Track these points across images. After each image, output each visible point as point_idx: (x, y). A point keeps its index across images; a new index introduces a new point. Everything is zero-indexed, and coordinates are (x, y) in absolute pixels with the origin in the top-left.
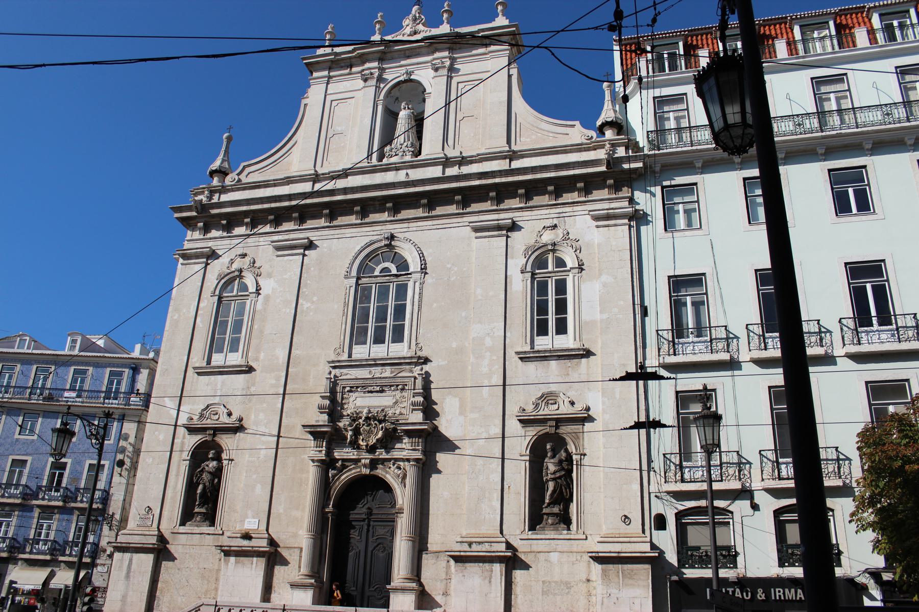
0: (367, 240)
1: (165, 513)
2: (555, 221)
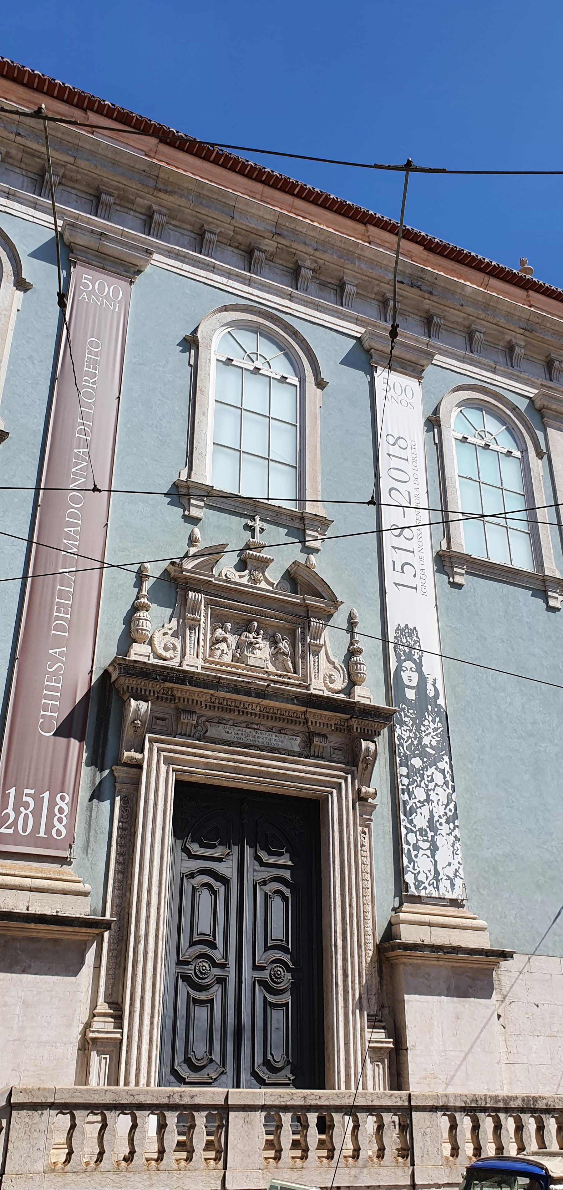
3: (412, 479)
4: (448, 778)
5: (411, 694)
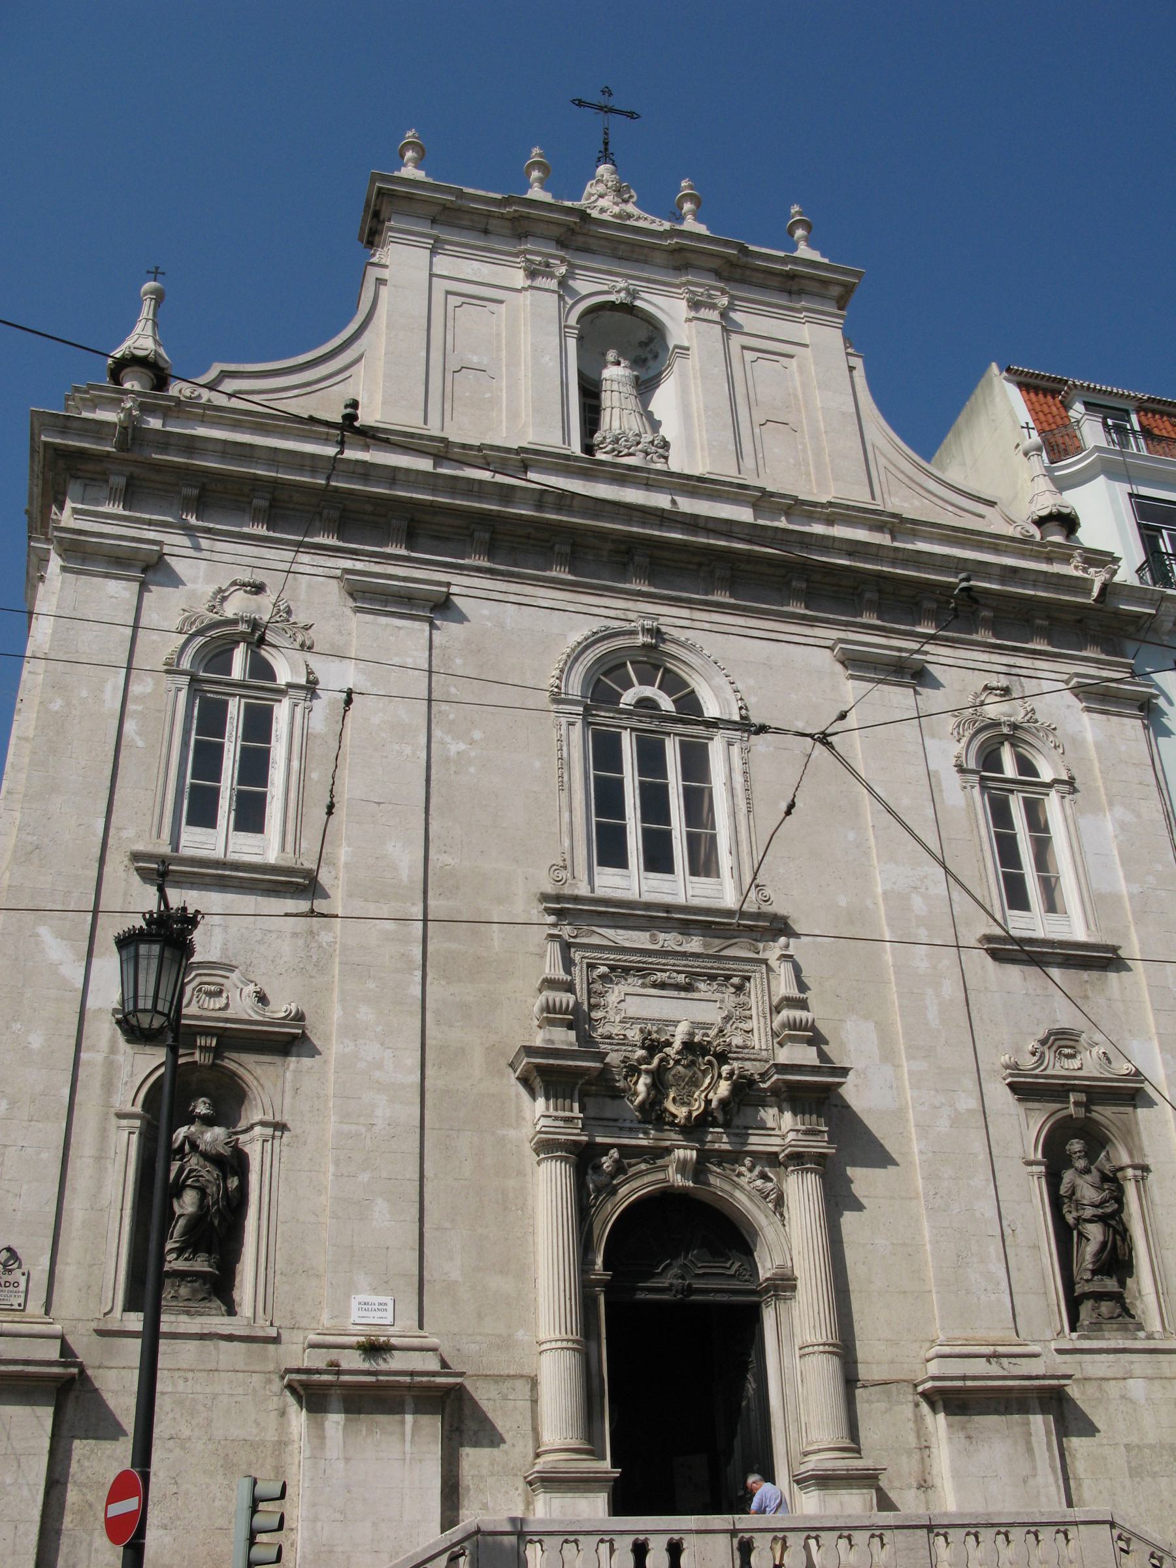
0: (596, 625)
1: (68, 1271)
2: (1003, 682)
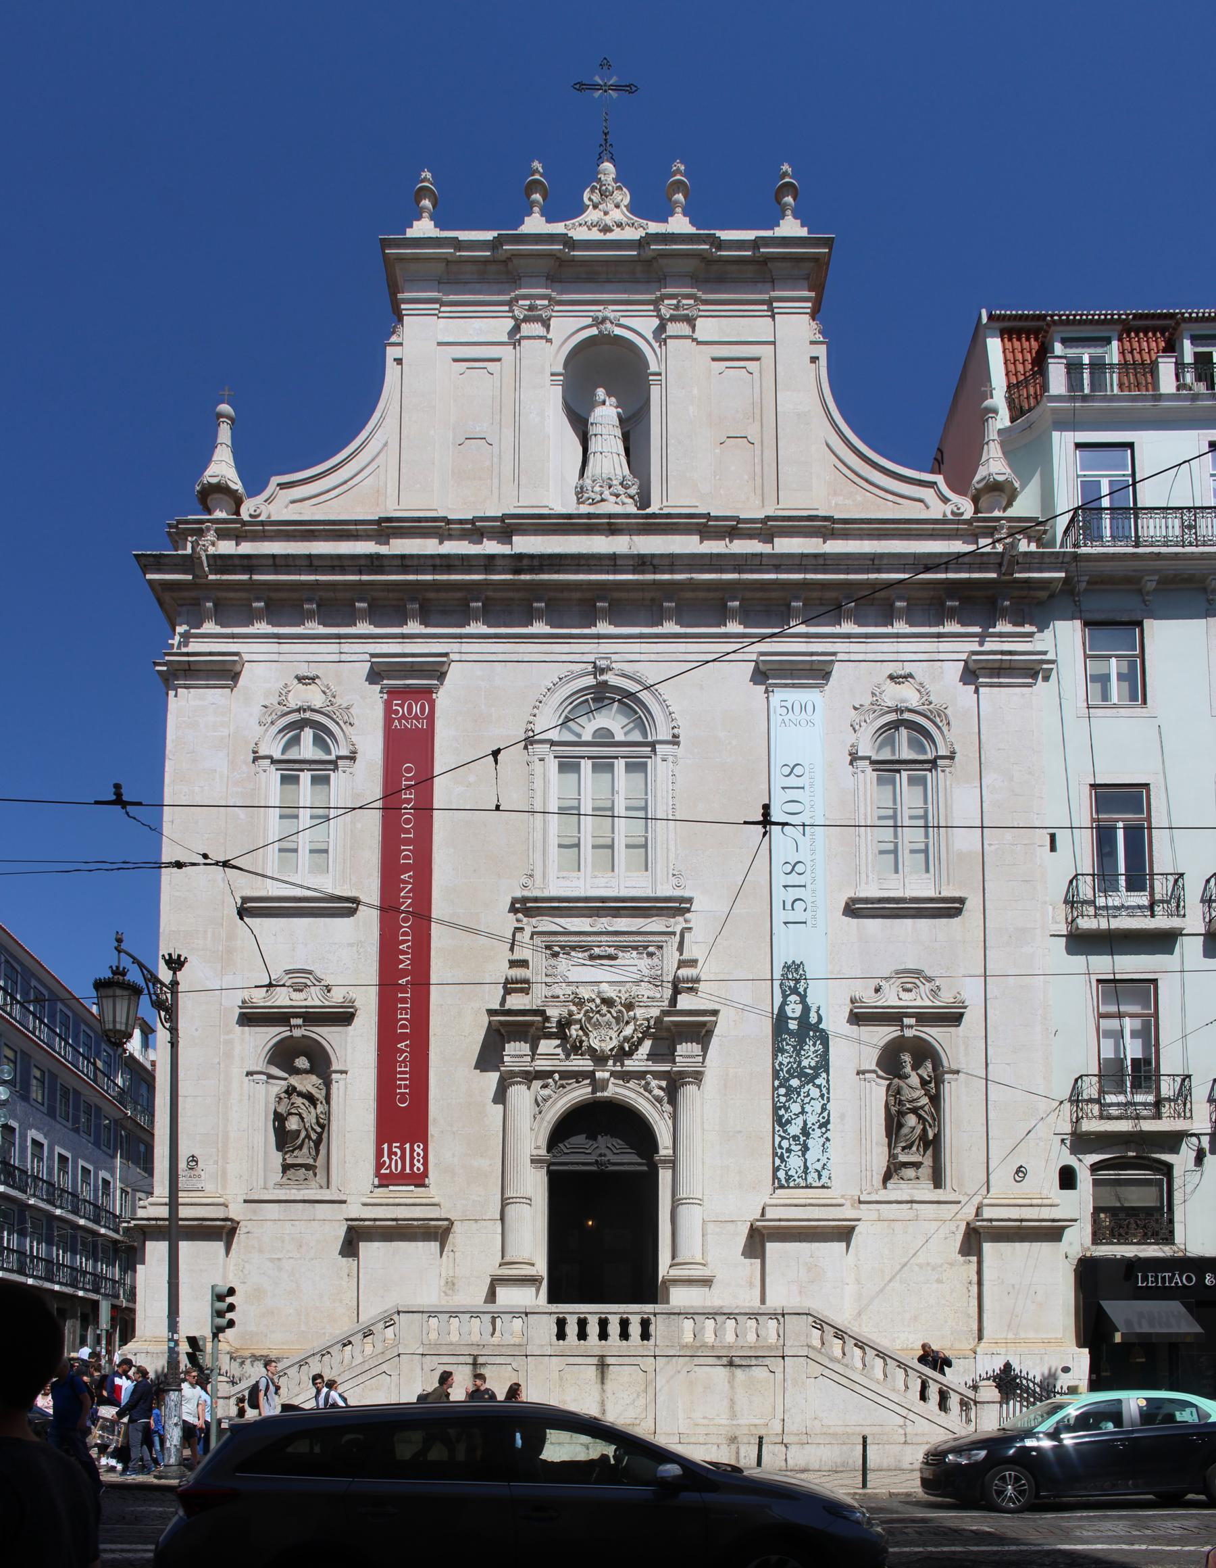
0: (563, 670)
3: (808, 806)
4: (824, 1091)
5: (793, 1025)
